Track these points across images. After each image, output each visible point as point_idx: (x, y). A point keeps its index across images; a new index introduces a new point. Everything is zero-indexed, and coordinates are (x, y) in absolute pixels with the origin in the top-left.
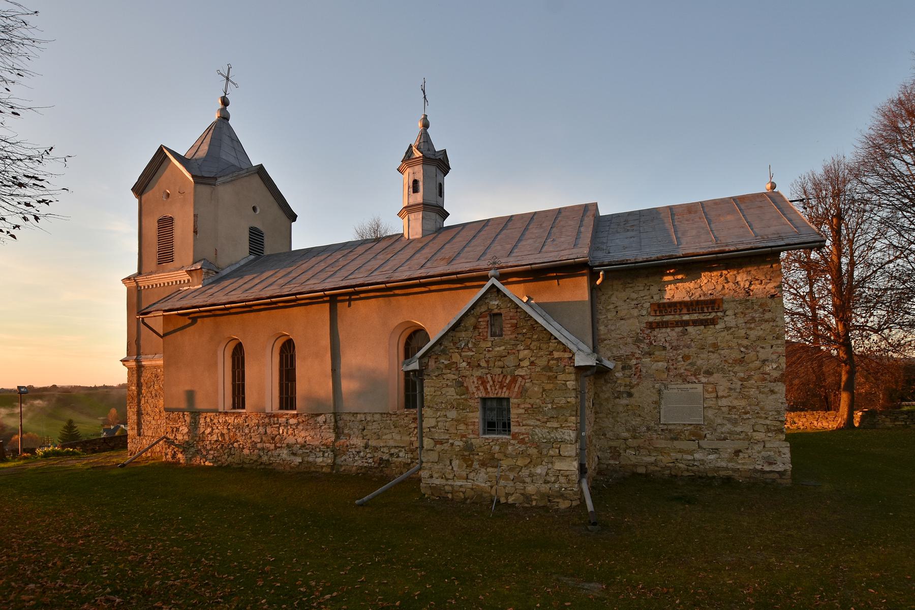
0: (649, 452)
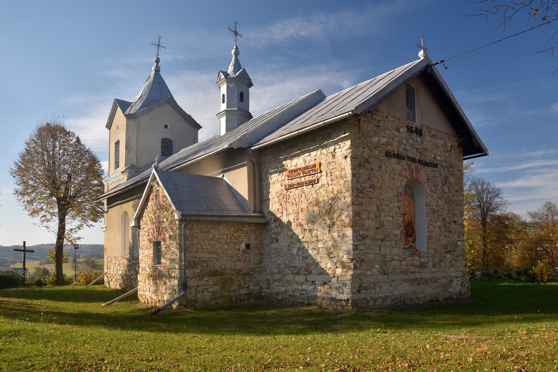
0: (284, 283)
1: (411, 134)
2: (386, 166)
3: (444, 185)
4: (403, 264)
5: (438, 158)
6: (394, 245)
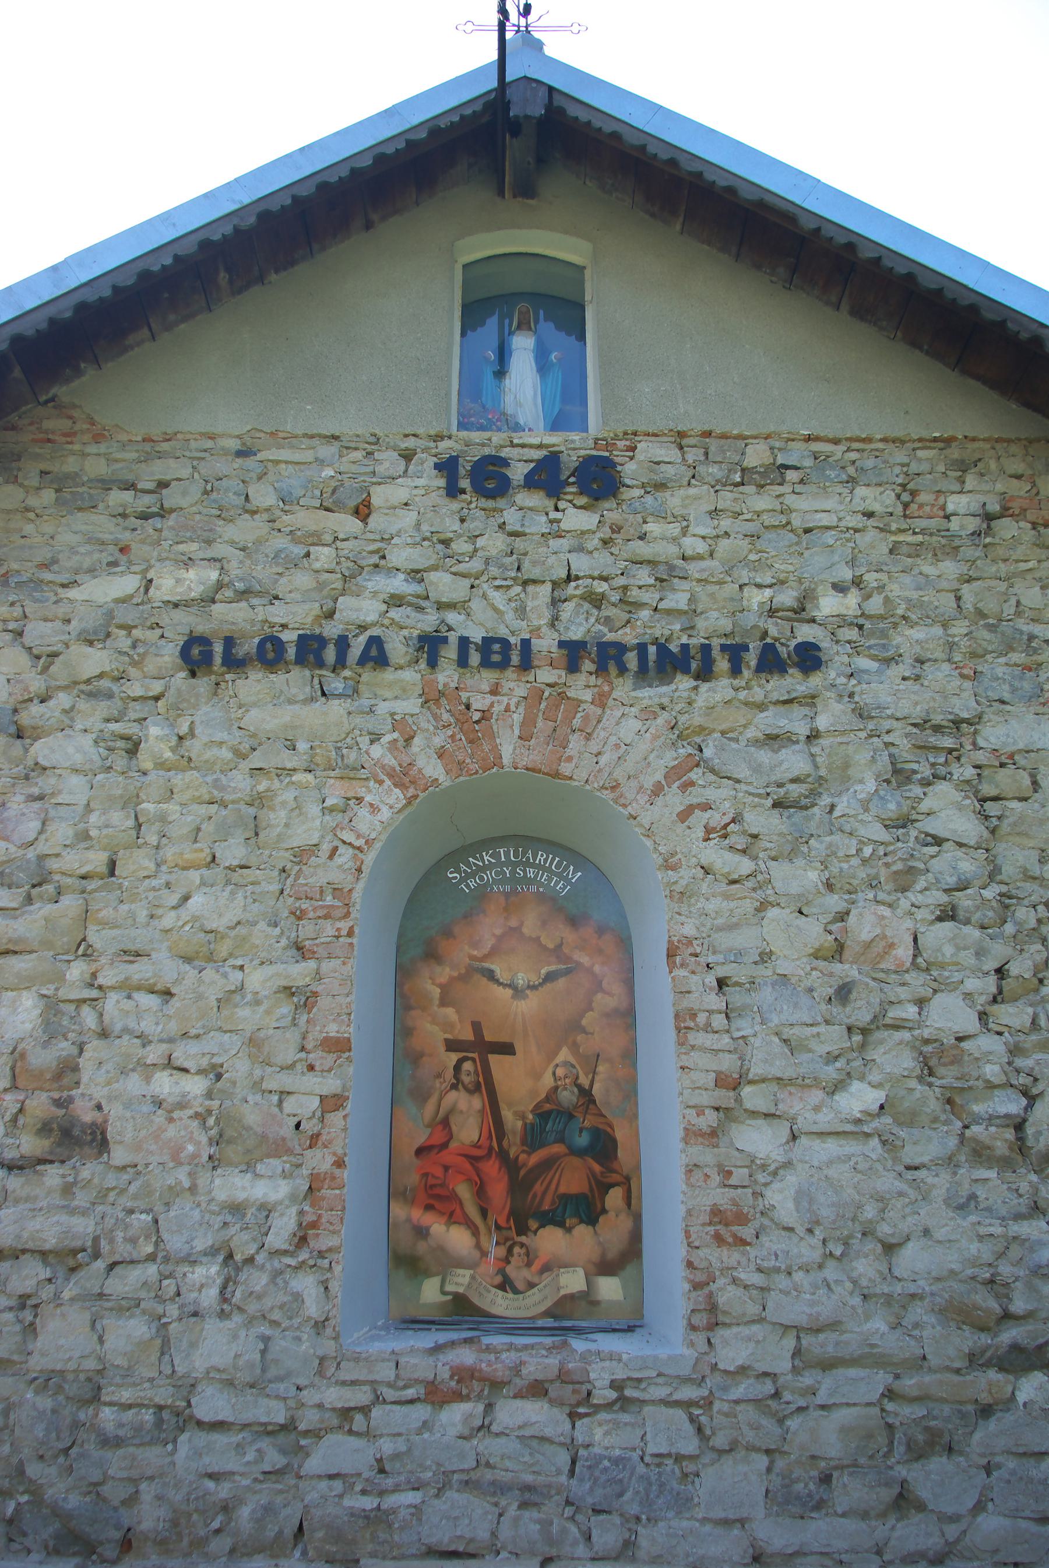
1: (501, 503)
2: (184, 729)
3: (926, 783)
4: (314, 1464)
5: (828, 605)
6: (210, 1297)
